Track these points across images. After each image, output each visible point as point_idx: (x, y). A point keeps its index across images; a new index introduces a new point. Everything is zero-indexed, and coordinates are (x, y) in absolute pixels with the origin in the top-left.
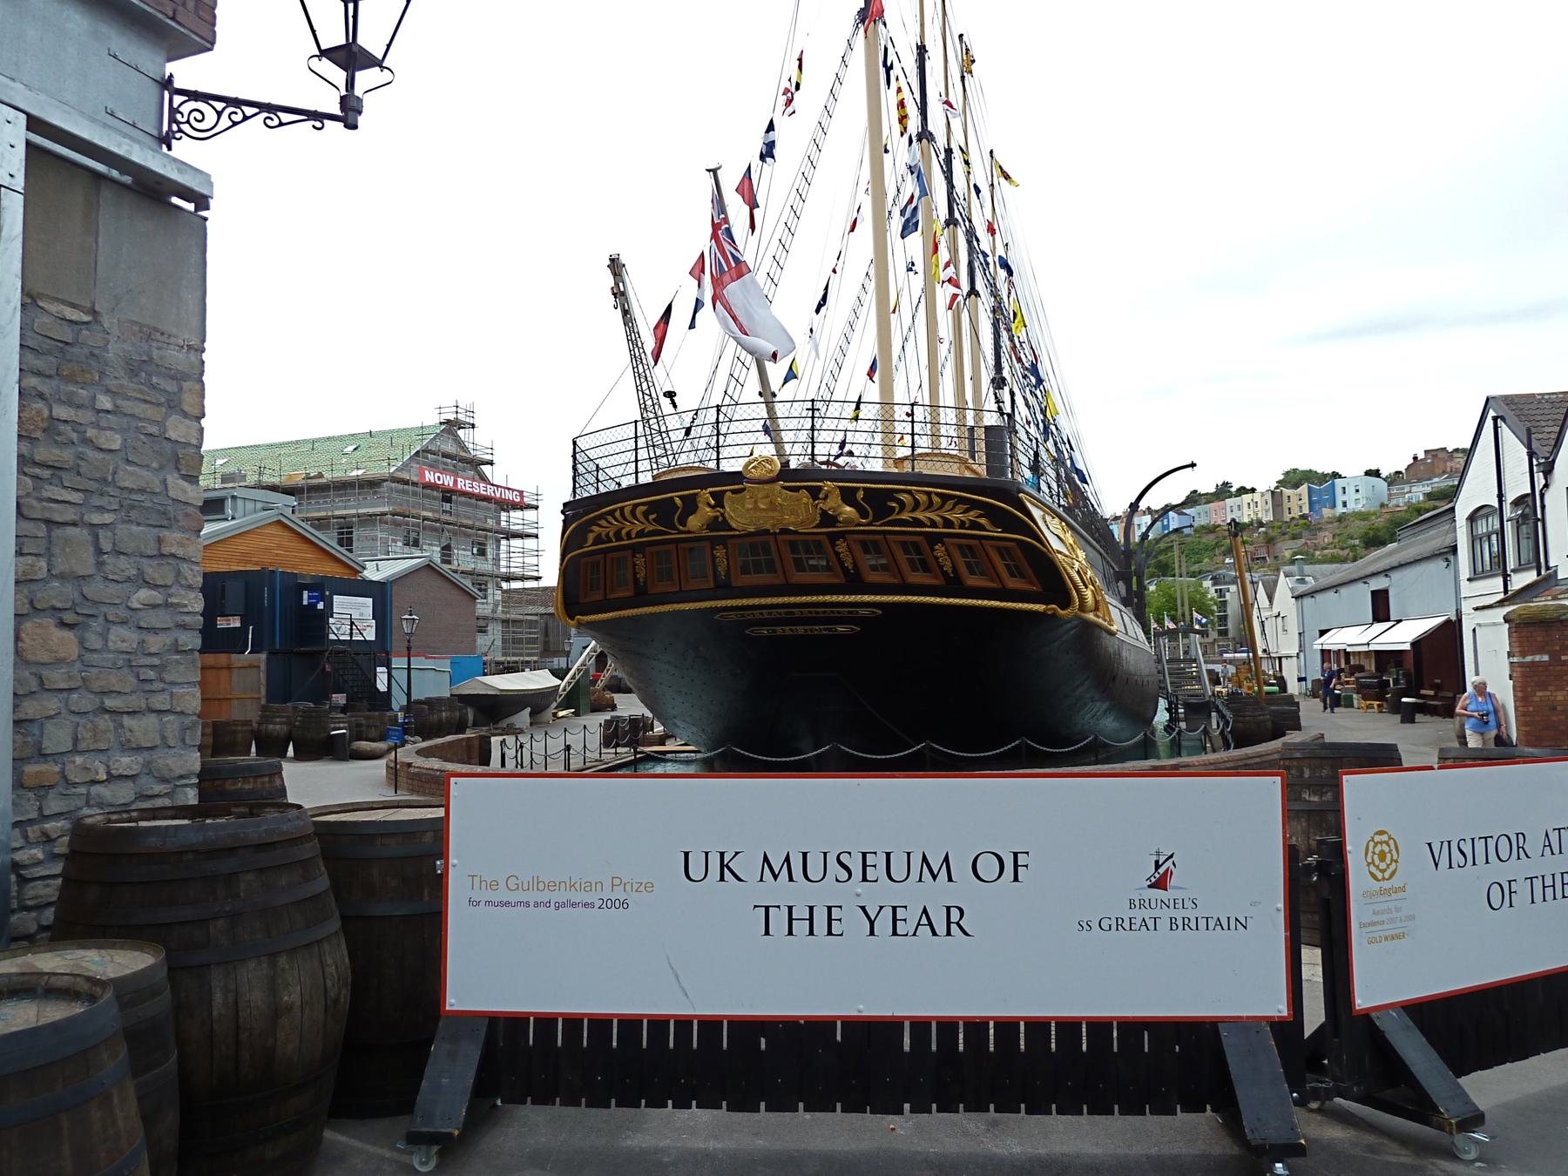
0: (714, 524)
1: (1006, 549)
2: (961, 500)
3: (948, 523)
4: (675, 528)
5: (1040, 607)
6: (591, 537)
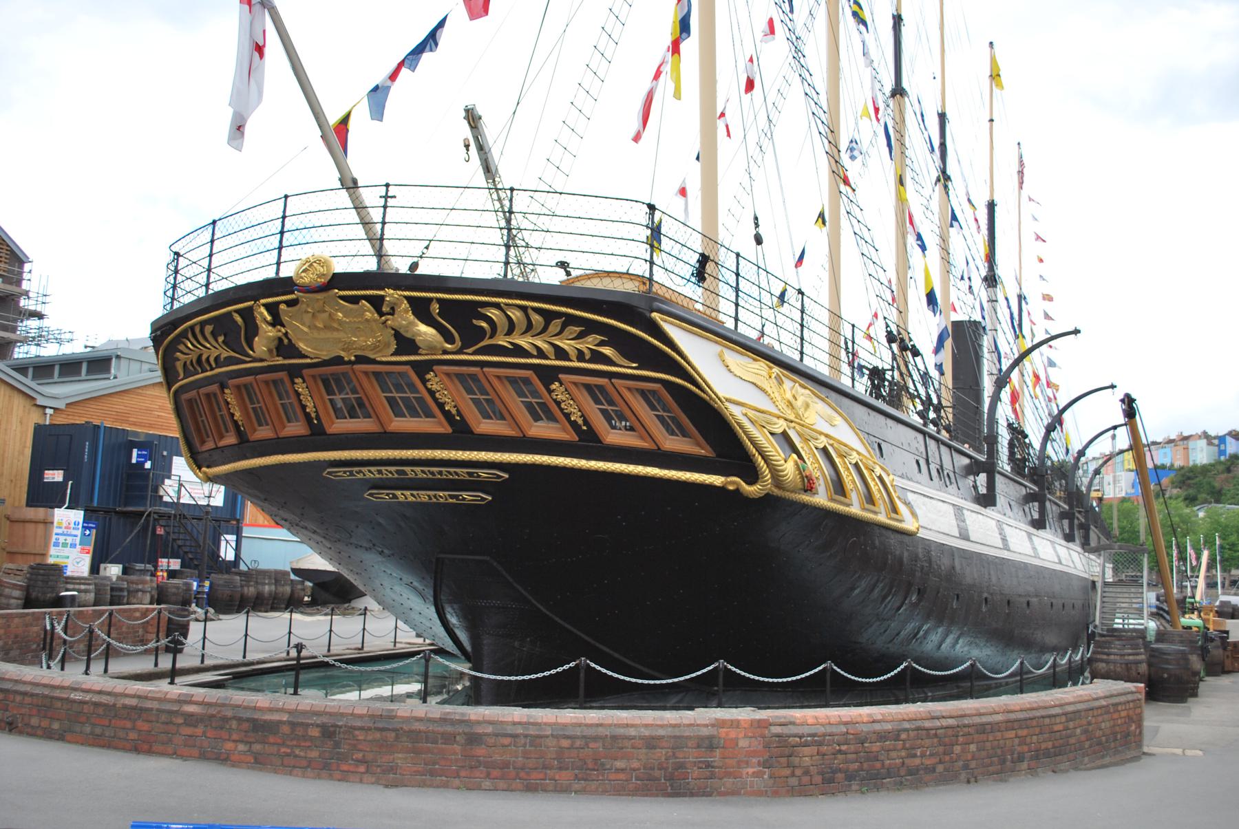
0: (285, 347)
1: (654, 392)
2: (570, 320)
3: (561, 353)
5: (717, 480)
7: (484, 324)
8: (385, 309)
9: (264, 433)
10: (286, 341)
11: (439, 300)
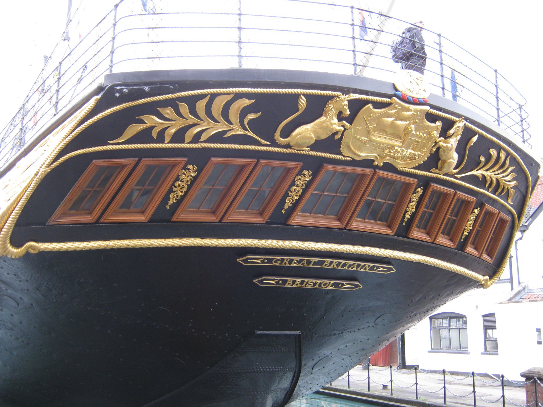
0: (332, 143)
6: (134, 129)
10: (337, 137)
11: (481, 137)
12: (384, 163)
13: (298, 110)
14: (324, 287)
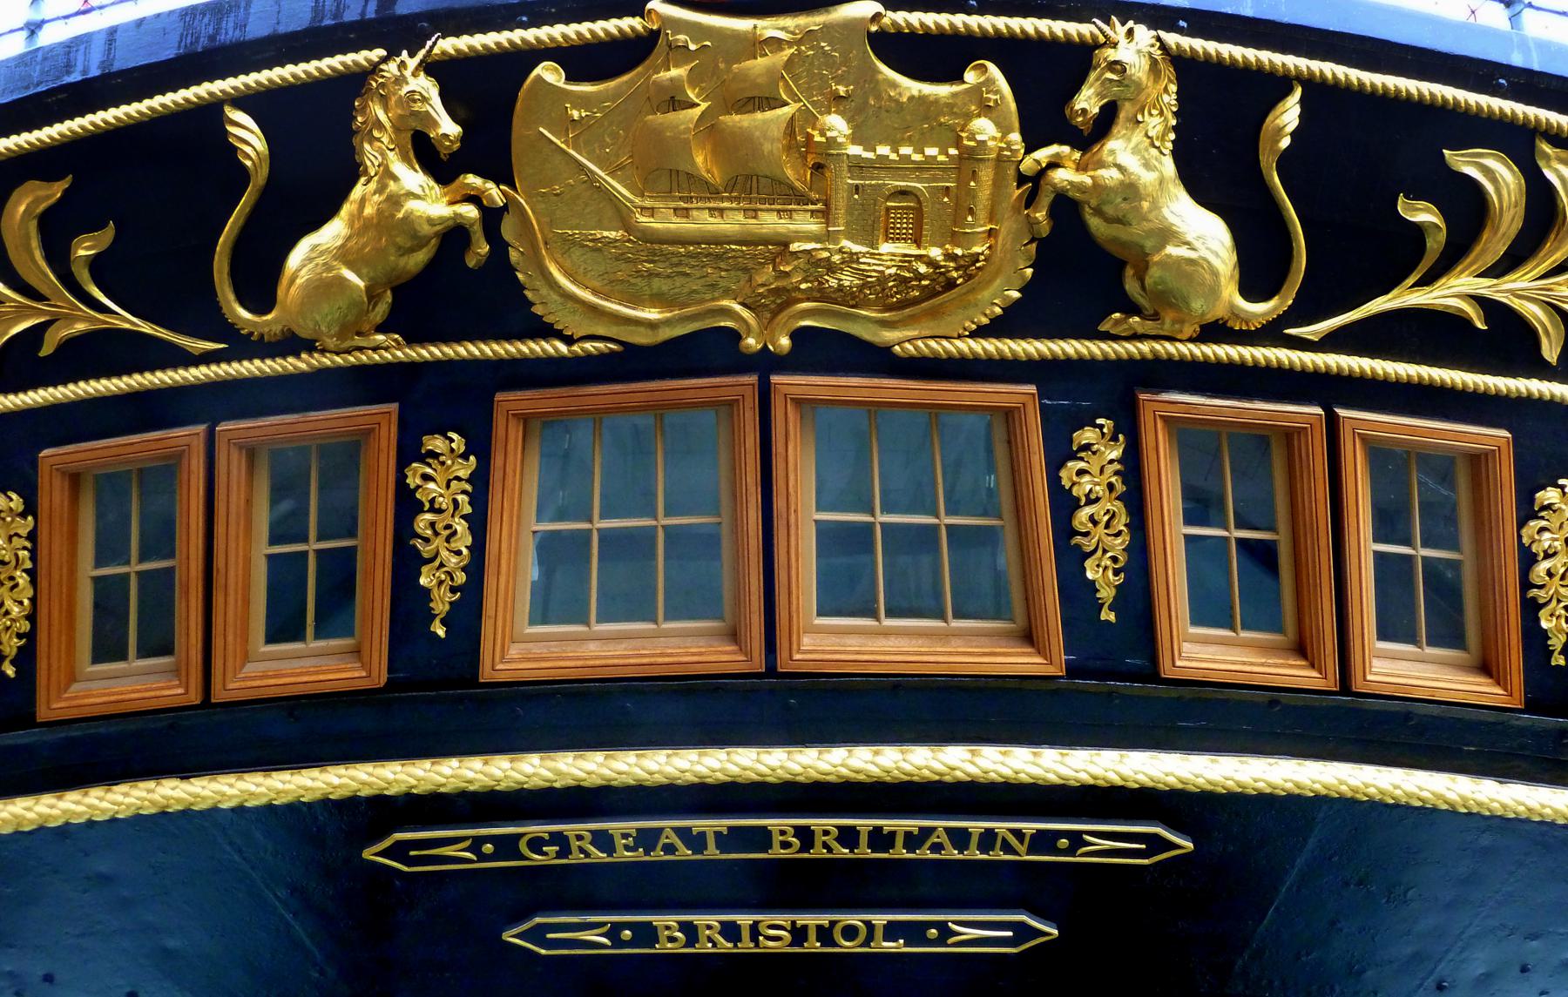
0: (455, 286)
4: (215, 325)
7: (1423, 214)
8: (1087, 101)
9: (139, 683)
11: (1318, 94)
12: (798, 335)
13: (243, 176)
14: (847, 946)
